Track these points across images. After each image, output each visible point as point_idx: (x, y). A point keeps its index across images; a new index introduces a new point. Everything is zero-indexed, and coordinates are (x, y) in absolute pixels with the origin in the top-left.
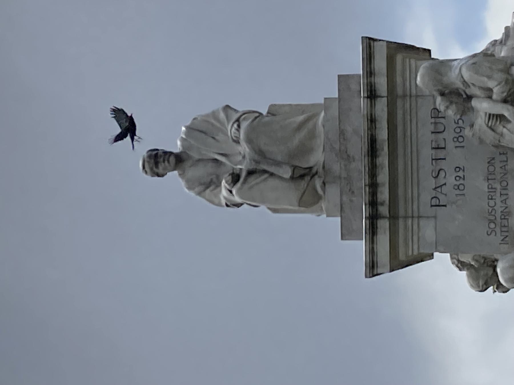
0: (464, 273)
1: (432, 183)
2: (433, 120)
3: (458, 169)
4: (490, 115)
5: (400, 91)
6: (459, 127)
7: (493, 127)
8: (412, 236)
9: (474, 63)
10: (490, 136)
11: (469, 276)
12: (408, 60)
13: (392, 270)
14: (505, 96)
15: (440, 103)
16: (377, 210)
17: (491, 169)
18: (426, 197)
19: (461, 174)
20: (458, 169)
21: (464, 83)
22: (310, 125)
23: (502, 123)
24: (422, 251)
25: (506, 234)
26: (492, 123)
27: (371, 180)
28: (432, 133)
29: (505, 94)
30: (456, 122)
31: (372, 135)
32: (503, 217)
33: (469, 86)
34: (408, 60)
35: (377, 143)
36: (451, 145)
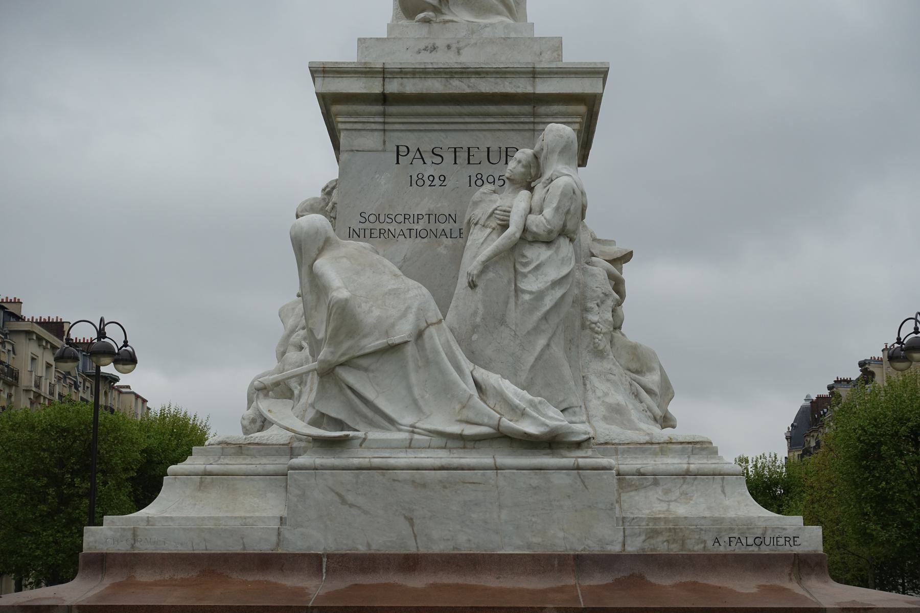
0: (319, 194)
1: (426, 147)
3: (442, 178)
4: (509, 212)
5: (542, 109)
6: (494, 181)
7: (494, 215)
9: (574, 193)
10: (481, 213)
11: (315, 199)
12: (579, 120)
13: (316, 93)
15: (524, 154)
17: (442, 219)
18: (411, 140)
20: (443, 178)
21: (550, 180)
22: (501, 8)
23: (498, 227)
24: (342, 134)
25: (362, 235)
26: (498, 214)
28: (488, 148)
29: (535, 229)
30: (501, 178)
33: (545, 187)
34: (579, 120)
36: (473, 170)
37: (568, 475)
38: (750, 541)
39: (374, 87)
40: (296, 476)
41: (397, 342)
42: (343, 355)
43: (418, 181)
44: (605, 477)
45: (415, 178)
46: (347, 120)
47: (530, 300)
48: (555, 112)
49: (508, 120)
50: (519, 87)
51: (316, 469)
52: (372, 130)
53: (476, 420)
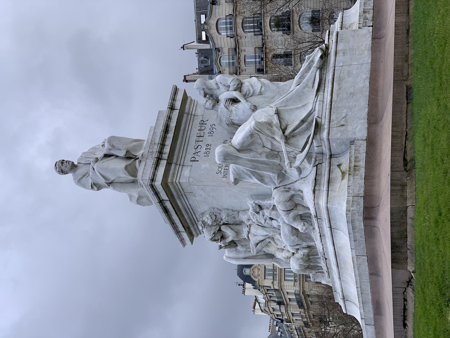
2: (200, 125)
3: (208, 145)
5: (187, 111)
14: (236, 87)
16: (162, 156)
18: (189, 157)
19: (209, 147)
23: (232, 105)
25: (227, 173)
27: (163, 142)
28: (198, 130)
29: (236, 86)
31: (168, 124)
32: (226, 166)
35: (170, 128)
36: (206, 135)
37: (339, 44)
39: (163, 163)
40: (332, 135)
41: (276, 139)
42: (279, 130)
43: (207, 154)
44: (341, 33)
47: (264, 87)
48: (188, 107)
50: (176, 114)
51: (329, 128)
52: (182, 170)
53: (313, 79)
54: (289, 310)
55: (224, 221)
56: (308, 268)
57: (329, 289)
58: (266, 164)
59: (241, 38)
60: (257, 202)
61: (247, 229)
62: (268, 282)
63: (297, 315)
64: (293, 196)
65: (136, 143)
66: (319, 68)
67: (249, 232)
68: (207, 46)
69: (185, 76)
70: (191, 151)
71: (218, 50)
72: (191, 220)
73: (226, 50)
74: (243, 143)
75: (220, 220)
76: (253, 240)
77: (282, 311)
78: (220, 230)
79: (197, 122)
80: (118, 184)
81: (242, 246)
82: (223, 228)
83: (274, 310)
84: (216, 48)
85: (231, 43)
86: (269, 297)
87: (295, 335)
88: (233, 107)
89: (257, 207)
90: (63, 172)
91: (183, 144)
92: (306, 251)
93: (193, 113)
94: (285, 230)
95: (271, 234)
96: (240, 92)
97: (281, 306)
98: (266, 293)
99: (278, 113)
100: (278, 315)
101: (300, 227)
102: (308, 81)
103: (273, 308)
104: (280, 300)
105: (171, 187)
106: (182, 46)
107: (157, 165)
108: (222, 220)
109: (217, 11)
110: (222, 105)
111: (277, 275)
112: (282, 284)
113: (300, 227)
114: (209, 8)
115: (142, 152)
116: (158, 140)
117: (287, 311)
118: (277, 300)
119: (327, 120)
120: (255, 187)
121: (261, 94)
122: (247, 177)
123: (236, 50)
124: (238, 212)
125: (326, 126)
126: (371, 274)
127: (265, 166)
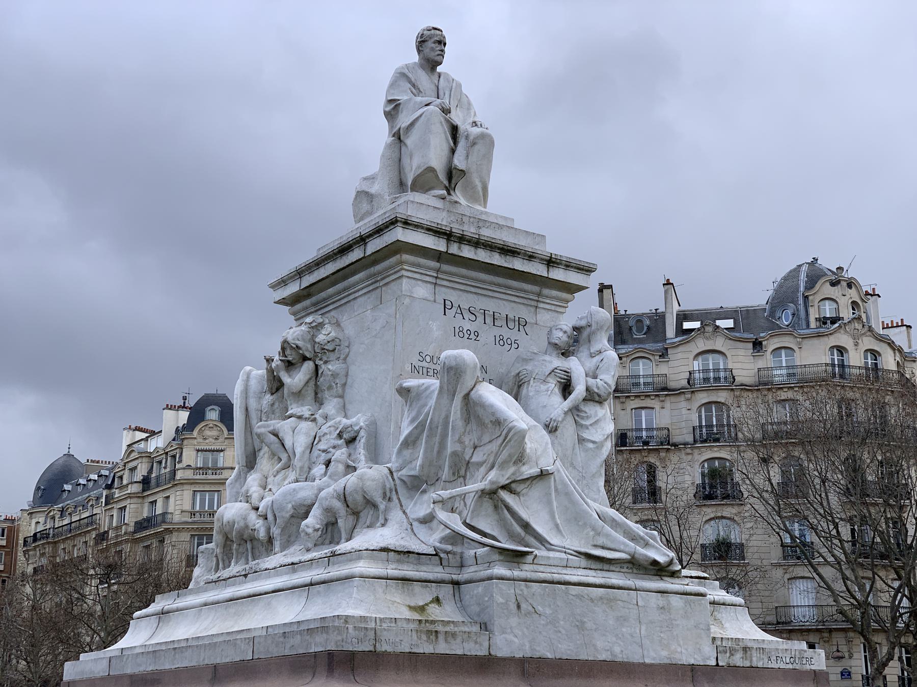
1: (465, 306)
2: (517, 319)
3: (476, 334)
5: (546, 291)
8: (421, 274)
14: (593, 390)
16: (455, 241)
18: (453, 297)
19: (472, 336)
23: (558, 383)
25: (421, 373)
27: (483, 244)
28: (507, 315)
29: (596, 390)
31: (519, 254)
32: (436, 371)
35: (511, 258)
36: (497, 331)
37: (681, 598)
38: (788, 661)
39: (440, 245)
40: (500, 586)
41: (491, 471)
42: (508, 479)
43: (459, 332)
45: (457, 330)
46: (410, 268)
47: (594, 448)
48: (554, 295)
49: (522, 295)
50: (538, 270)
51: (514, 580)
52: (426, 282)
53: (612, 546)
54: (133, 501)
55: (323, 366)
56: (227, 540)
57: (182, 584)
58: (439, 452)
59: (688, 400)
60: (362, 433)
61: (307, 414)
62: (189, 457)
63: (122, 517)
64: (375, 506)
65: (480, 188)
66: (633, 557)
67: (300, 417)
68: (670, 331)
69: (610, 287)
70: (465, 301)
71: (664, 354)
72: (325, 300)
73: (663, 369)
74: (482, 405)
75: (325, 358)
76: (285, 427)
77: (130, 486)
78: (305, 359)
79: (524, 313)
80: (397, 154)
81: (273, 405)
82: (308, 366)
83: (133, 470)
84: (667, 349)
85: (678, 379)
86: (158, 459)
87: (80, 514)
88: (553, 385)
89: (352, 434)
90: (422, 42)
91: (478, 285)
92: (262, 534)
93: (541, 305)
94: (305, 491)
95: (296, 462)
96: (584, 400)
97: (141, 485)
98: (167, 453)
99: (543, 475)
100: (121, 478)
101: (312, 521)
102: (608, 536)
103: (136, 468)
104: (153, 482)
105: (393, 260)
106: (671, 281)
107: (437, 232)
108: (326, 362)
109: (742, 352)
110: (557, 362)
111: (204, 477)
112: (186, 487)
113: (312, 521)
114: (746, 335)
115: (463, 201)
116: (487, 233)
117: (130, 496)
118: (153, 475)
119: (529, 575)
120: (392, 429)
121: (581, 440)
122: (413, 414)
123: (664, 390)
124: (341, 397)
125: (516, 573)
126: (215, 667)
127: (436, 449)
